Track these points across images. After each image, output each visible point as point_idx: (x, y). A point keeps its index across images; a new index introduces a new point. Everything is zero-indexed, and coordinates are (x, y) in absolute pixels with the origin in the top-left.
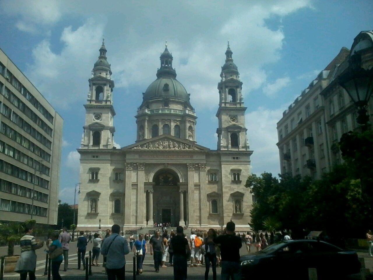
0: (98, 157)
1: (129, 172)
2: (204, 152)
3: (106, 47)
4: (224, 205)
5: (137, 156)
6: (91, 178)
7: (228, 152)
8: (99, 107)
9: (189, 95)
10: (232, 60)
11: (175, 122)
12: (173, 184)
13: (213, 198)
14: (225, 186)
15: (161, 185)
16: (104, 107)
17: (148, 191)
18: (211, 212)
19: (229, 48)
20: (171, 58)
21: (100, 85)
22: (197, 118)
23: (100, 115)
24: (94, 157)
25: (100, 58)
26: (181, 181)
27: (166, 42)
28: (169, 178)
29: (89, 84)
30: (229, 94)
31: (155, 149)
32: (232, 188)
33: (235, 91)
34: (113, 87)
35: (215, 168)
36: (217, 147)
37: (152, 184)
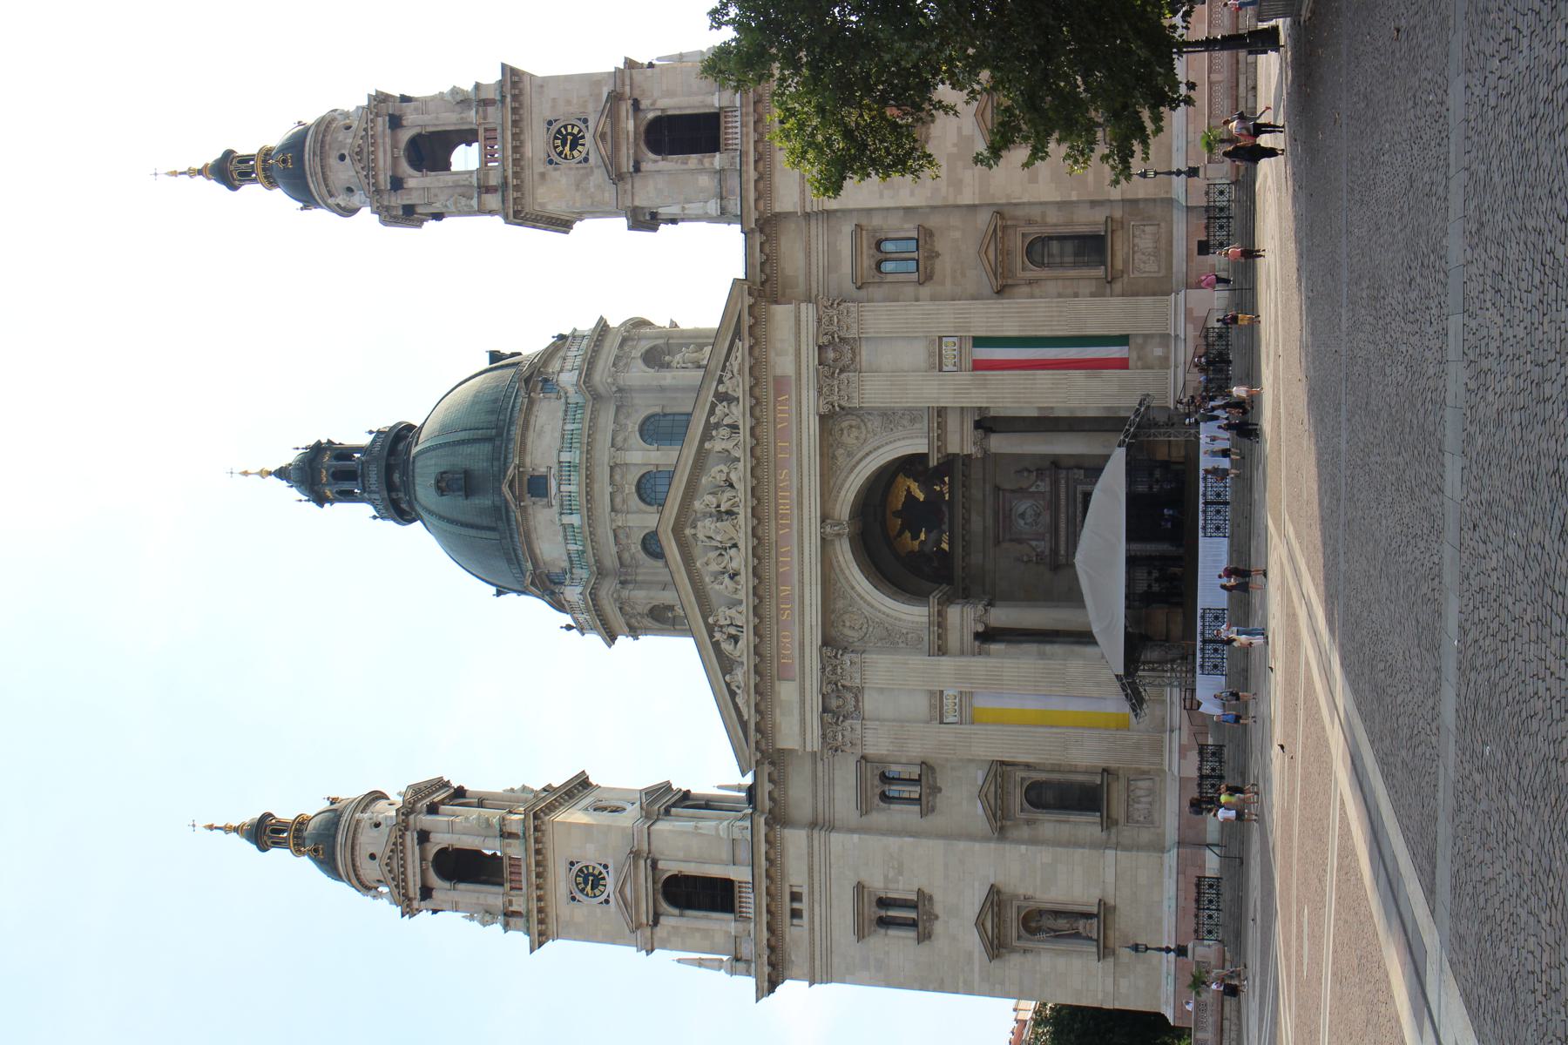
0: (795, 889)
1: (870, 738)
2: (750, 307)
3: (251, 815)
4: (1059, 199)
5: (787, 691)
6: (912, 934)
7: (752, 174)
8: (538, 875)
9: (495, 356)
10: (266, 154)
11: (625, 440)
12: (946, 479)
13: (1019, 258)
14: (944, 190)
15: (951, 543)
16: (538, 852)
17: (978, 636)
18: (1100, 272)
19: (200, 172)
20: (317, 450)
21: (431, 857)
22: (601, 318)
23: (581, 870)
24: (796, 914)
25: (298, 852)
26: (919, 446)
27: (245, 473)
28: (909, 495)
29: (425, 915)
30: (446, 166)
31: (742, 595)
32: (955, 145)
33: (419, 135)
34: (447, 785)
35: (845, 247)
36: (732, 225)
37: (940, 614)
